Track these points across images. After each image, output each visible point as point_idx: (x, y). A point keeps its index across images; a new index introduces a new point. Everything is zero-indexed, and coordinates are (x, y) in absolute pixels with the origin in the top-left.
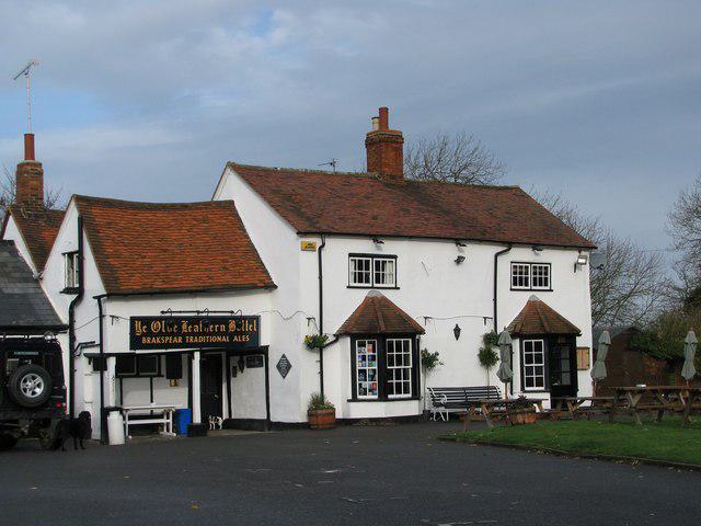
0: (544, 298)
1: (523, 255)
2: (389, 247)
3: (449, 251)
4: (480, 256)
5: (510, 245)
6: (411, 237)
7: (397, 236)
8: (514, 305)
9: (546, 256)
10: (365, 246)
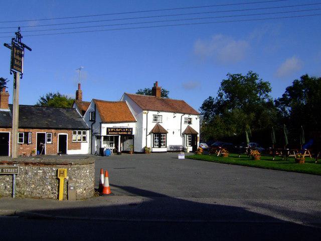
0: (190, 125)
1: (187, 116)
2: (161, 113)
3: (172, 114)
4: (179, 115)
5: (184, 114)
6: (165, 112)
7: (163, 111)
8: (185, 126)
9: (191, 116)
10: (156, 113)
